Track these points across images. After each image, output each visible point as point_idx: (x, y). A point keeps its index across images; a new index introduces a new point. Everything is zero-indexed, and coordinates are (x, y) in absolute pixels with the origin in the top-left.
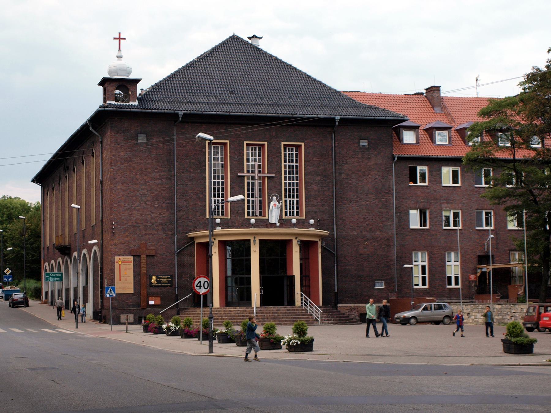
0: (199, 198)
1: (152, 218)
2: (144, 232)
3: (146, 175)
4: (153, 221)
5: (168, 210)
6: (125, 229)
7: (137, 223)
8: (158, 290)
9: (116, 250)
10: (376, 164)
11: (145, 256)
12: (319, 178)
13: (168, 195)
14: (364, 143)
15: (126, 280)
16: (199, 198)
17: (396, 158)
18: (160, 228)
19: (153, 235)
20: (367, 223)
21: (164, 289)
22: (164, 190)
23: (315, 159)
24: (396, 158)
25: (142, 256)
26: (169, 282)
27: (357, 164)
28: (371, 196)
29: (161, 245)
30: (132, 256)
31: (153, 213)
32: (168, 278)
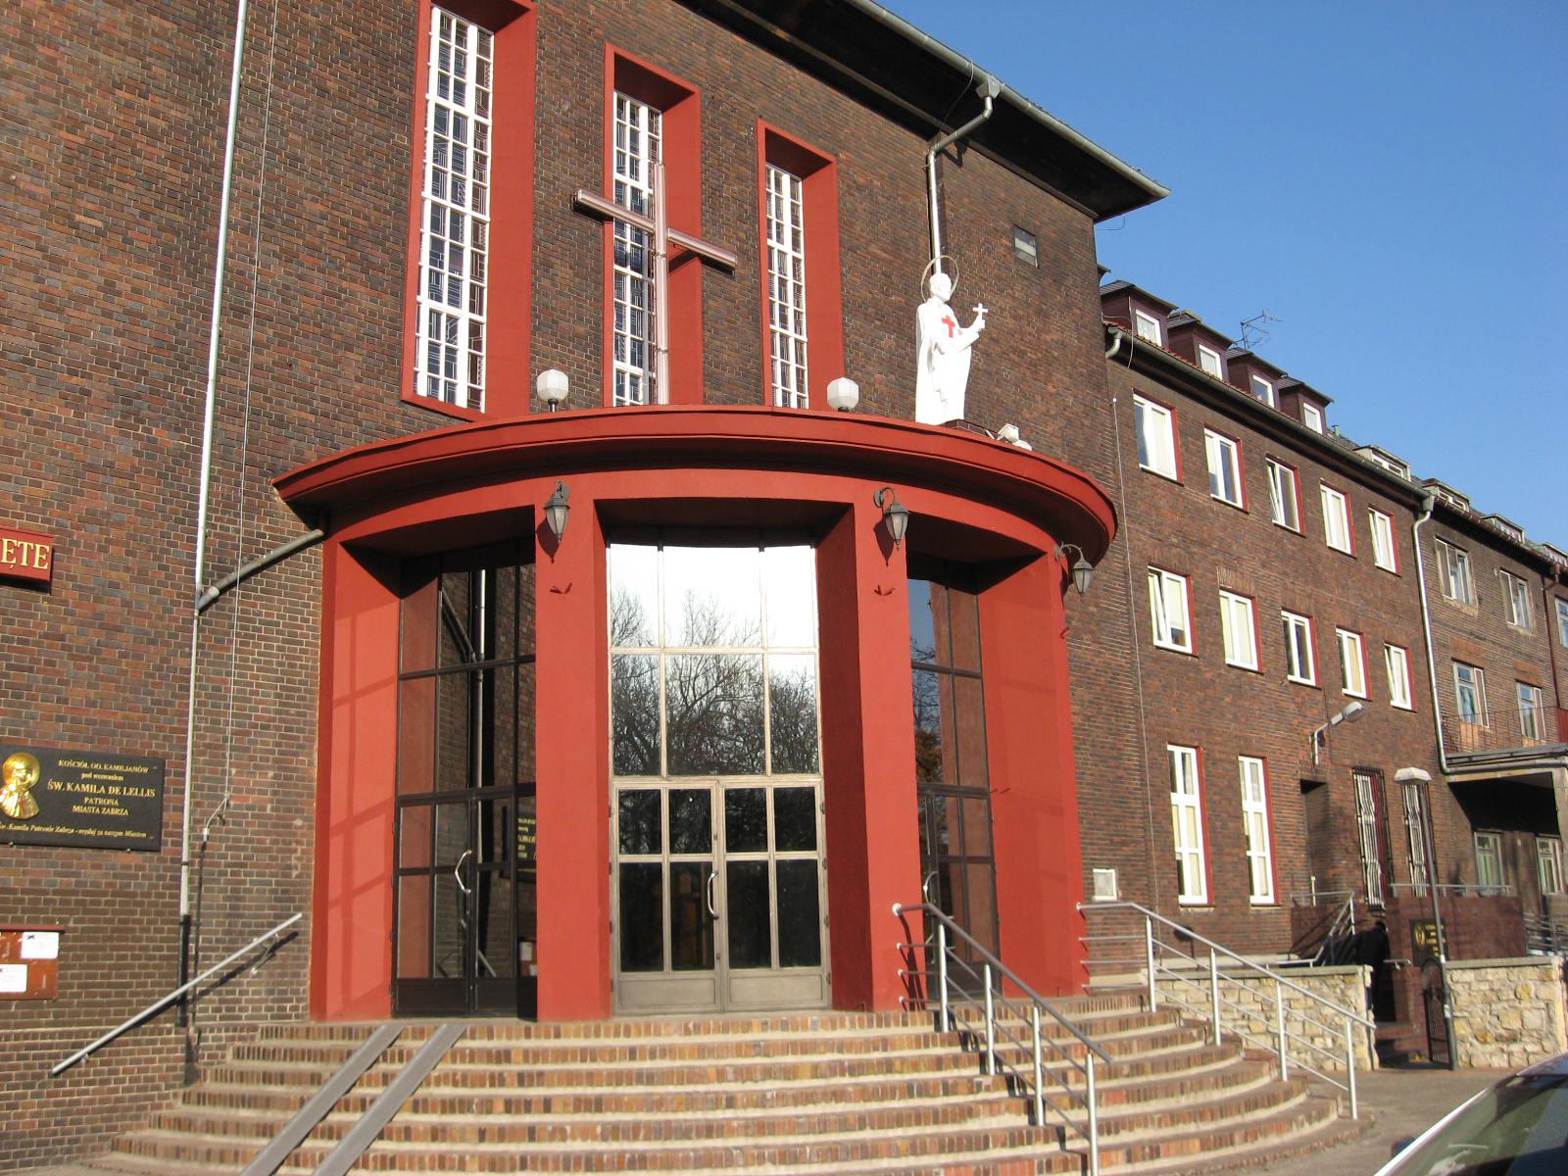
0: (366, 265)
1: (48, 303)
4: (53, 322)
5: (166, 272)
8: (46, 870)
13: (177, 176)
14: (1027, 249)
16: (366, 265)
17: (1117, 343)
19: (42, 426)
21: (92, 869)
22: (154, 135)
23: (874, 249)
24: (1117, 343)
29: (91, 518)
31: (57, 263)
32: (130, 780)
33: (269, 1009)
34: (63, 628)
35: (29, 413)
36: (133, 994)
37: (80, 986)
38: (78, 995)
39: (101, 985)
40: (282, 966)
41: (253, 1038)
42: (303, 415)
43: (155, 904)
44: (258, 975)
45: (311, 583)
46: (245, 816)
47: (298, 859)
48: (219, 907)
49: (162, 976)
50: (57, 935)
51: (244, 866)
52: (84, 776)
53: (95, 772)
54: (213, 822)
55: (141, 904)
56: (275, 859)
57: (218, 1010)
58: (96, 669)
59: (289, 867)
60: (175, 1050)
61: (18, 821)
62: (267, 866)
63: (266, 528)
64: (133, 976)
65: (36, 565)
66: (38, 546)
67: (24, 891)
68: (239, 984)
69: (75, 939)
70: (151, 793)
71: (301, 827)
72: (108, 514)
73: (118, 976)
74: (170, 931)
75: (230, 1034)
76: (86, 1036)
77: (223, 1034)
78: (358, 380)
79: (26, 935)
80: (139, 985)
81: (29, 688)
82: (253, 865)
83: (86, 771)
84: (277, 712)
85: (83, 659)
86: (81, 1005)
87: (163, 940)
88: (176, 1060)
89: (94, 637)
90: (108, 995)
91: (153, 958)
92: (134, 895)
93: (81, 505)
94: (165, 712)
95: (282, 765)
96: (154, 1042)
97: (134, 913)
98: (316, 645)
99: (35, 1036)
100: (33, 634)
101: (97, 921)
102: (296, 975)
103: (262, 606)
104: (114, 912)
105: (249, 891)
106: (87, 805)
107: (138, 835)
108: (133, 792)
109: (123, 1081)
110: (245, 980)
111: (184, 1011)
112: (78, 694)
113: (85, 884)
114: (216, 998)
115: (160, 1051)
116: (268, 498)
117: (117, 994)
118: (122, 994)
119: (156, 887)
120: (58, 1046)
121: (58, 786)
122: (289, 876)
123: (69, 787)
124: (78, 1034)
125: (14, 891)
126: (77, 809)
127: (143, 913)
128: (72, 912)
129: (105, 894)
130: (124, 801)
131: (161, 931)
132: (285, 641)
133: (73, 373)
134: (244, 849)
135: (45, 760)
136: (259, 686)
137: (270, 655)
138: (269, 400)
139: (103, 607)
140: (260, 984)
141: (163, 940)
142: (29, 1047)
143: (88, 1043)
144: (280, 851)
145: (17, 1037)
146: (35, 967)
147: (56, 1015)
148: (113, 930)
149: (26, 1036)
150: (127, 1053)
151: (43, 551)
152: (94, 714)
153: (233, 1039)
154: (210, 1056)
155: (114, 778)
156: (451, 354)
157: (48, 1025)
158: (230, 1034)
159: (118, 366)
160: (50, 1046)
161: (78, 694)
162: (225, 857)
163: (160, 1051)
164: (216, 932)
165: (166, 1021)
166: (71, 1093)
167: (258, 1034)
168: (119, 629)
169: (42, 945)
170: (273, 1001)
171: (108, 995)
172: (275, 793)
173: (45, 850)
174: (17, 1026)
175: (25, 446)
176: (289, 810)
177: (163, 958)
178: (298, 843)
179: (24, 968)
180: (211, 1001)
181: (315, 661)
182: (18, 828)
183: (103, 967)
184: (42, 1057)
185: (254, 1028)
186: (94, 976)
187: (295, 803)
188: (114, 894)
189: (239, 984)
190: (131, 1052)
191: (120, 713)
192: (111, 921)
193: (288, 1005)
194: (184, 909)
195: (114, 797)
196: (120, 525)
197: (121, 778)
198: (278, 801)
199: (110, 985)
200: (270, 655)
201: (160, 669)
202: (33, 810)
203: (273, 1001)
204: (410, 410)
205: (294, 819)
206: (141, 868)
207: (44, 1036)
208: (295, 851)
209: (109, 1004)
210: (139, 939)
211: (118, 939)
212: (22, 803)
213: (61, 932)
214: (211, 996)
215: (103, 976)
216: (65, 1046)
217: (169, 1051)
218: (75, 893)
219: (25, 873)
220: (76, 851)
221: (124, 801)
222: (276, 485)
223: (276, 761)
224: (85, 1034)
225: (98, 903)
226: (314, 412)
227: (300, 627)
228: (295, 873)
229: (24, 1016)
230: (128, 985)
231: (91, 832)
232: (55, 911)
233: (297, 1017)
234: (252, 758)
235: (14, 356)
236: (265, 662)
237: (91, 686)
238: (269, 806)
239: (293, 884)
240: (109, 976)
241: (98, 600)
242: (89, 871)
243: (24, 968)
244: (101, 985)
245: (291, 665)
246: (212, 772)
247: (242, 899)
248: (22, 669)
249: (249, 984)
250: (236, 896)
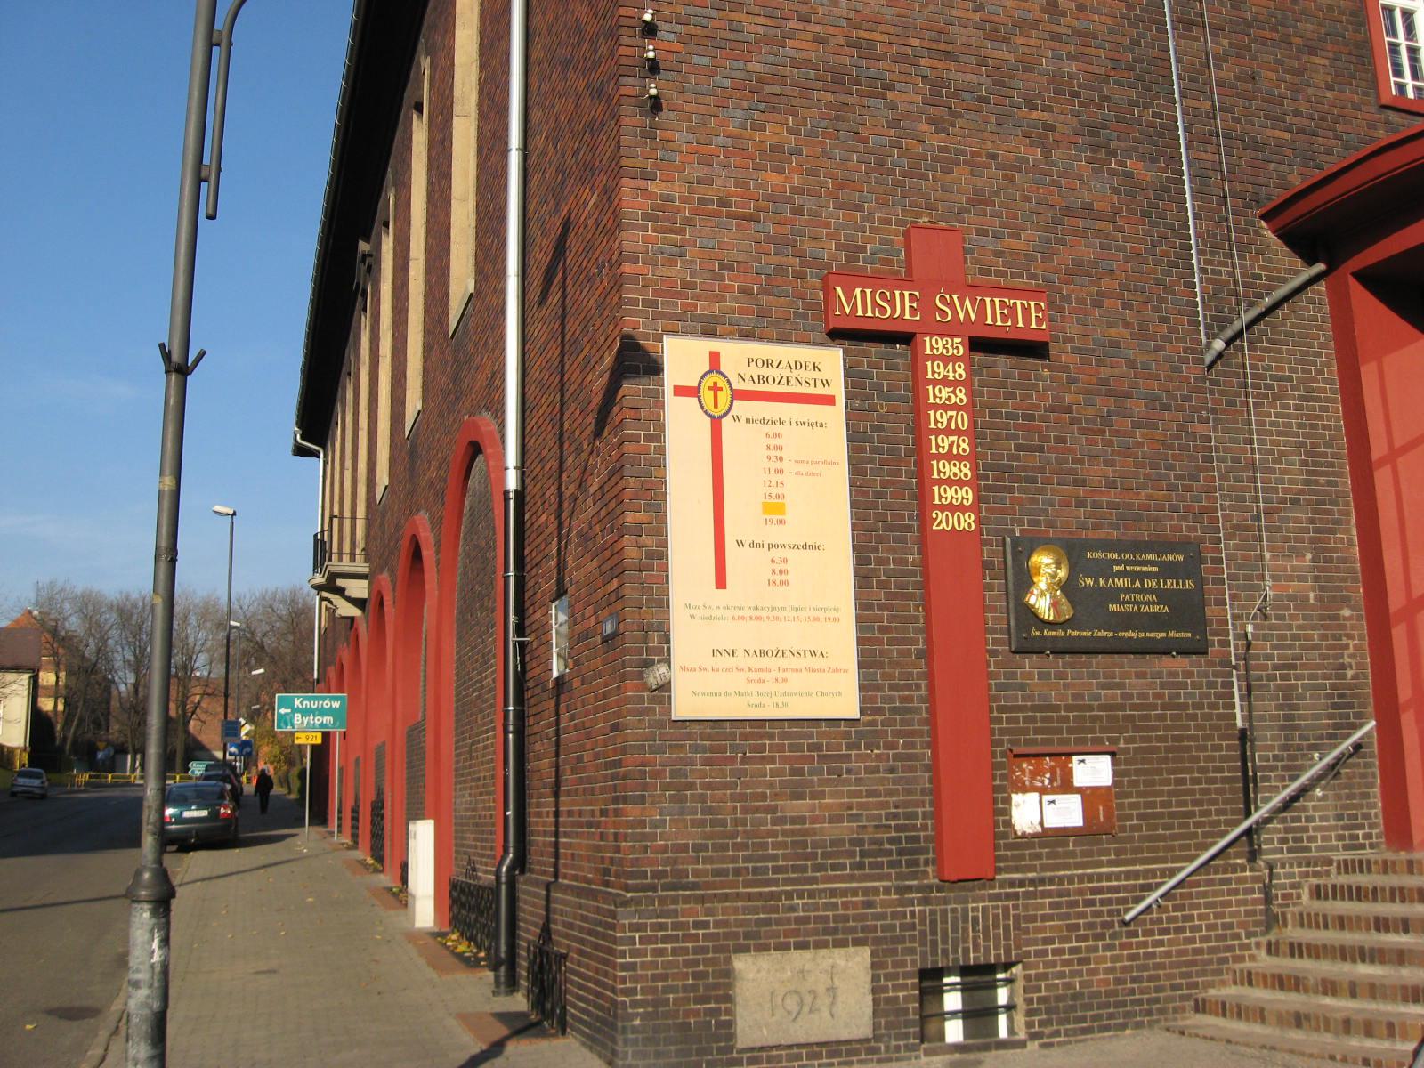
2: (934, 140)
4: (1003, 53)
6: (754, 88)
7: (868, 51)
8: (1088, 681)
9: (678, 273)
15: (779, 578)
18: (1064, 123)
25: (934, 344)
29: (1077, 270)
30: (837, 335)
32: (1168, 571)
33: (1341, 838)
34: (1068, 398)
35: (993, 157)
36: (1198, 825)
37: (1141, 817)
38: (1138, 828)
39: (1161, 816)
40: (1346, 786)
41: (1328, 873)
42: (1277, 133)
43: (1209, 717)
44: (1324, 798)
45: (1320, 328)
46: (1287, 608)
47: (1351, 656)
48: (1273, 718)
49: (1226, 802)
50: (1107, 758)
51: (1294, 667)
52: (1116, 568)
53: (1127, 563)
54: (1255, 617)
55: (1194, 718)
56: (1326, 657)
57: (1284, 841)
58: (1110, 443)
59: (1343, 667)
60: (1252, 891)
61: (1052, 625)
62: (1318, 667)
63: (1261, 268)
64: (1196, 803)
65: (1034, 326)
66: (1032, 304)
67: (1068, 708)
68: (1304, 809)
69: (1127, 762)
70: (1190, 585)
71: (1350, 618)
72: (1094, 264)
73: (1180, 804)
74: (1229, 748)
75: (1303, 869)
76: (1154, 877)
77: (1296, 870)
78: (1330, 88)
79: (1075, 758)
80: (1203, 814)
81: (1042, 470)
82: (1303, 666)
83: (1118, 563)
84: (1306, 482)
85: (1095, 433)
86: (1142, 839)
87: (1223, 759)
88: (1255, 902)
89: (1103, 405)
90: (1170, 827)
91: (1214, 781)
92: (1185, 707)
93: (1065, 256)
94: (1190, 489)
95: (1318, 545)
96: (1228, 881)
97: (1187, 728)
98: (1334, 401)
99: (1100, 877)
100: (1038, 407)
101: (1149, 739)
102: (1366, 796)
103: (1271, 359)
104: (1167, 728)
105: (1303, 697)
106: (1124, 602)
107: (1183, 635)
108: (1170, 584)
109: (1199, 928)
110: (1310, 804)
111: (1251, 843)
112: (1096, 472)
113: (1130, 696)
114: (1281, 826)
115: (1236, 892)
116: (1257, 233)
117: (1181, 826)
118: (1186, 826)
119: (1208, 696)
120: (1126, 889)
121: (1090, 582)
122: (1344, 677)
123: (1102, 582)
124: (1147, 874)
125: (1056, 708)
126: (1113, 608)
127: (1198, 728)
128: (1120, 730)
129: (1154, 707)
131: (1219, 748)
132: (1302, 398)
133: (1032, 108)
134: (1291, 647)
135: (1072, 552)
136: (1281, 453)
137: (1288, 416)
138: (1238, 120)
139: (1106, 371)
140: (1326, 808)
141: (1223, 759)
142: (1095, 891)
143: (1159, 885)
144: (1330, 648)
145: (1081, 879)
146: (1091, 796)
147: (1118, 852)
148: (1168, 750)
149: (1090, 878)
150: (1200, 895)
151: (1038, 307)
152: (1114, 495)
153: (1307, 875)
154: (1285, 897)
155: (1149, 569)
157: (1111, 863)
158: (1303, 869)
159: (1077, 95)
160: (1116, 890)
161: (1096, 472)
162: (1271, 658)
163: (1236, 892)
164: (1272, 748)
165: (1237, 856)
166: (1145, 944)
167: (1333, 869)
168: (1128, 395)
169: (1094, 771)
170: (1343, 828)
171: (1170, 827)
172: (1316, 579)
173: (1084, 658)
174: (1078, 866)
175: (996, 194)
176: (1334, 598)
177: (1224, 780)
178: (1350, 637)
179: (1077, 798)
180: (1277, 831)
181: (1337, 420)
182: (1054, 634)
183: (1160, 793)
184: (1110, 902)
185: (1329, 862)
186: (1153, 805)
187: (1339, 589)
188: (1164, 707)
189: (1304, 809)
190: (1205, 894)
191: (1143, 493)
192: (1163, 739)
193: (1361, 833)
194: (1239, 723)
195: (1151, 591)
196: (1110, 274)
197: (1156, 569)
198: (1322, 589)
199: (1172, 815)
200: (1288, 416)
201: (1178, 438)
202: (1067, 612)
203: (1343, 828)
204: (1392, 116)
205: (1340, 608)
206: (1189, 674)
207: (1109, 877)
208: (1346, 647)
209: (1174, 837)
210: (1197, 759)
211: (1175, 760)
212: (1055, 605)
213: (1113, 754)
214: (1275, 825)
215: (1163, 804)
216: (1134, 888)
217: (1246, 891)
218: (1122, 707)
219: (1066, 686)
220: (1117, 658)
222: (1263, 217)
223: (1312, 540)
224: (1153, 873)
225: (1147, 718)
226: (1288, 130)
227: (1315, 381)
228: (1350, 673)
229: (1083, 854)
230: (1190, 814)
231: (1131, 634)
232: (1104, 729)
233: (1372, 846)
234: (1287, 539)
235: (967, 95)
236: (1285, 425)
237: (1108, 463)
238: (1312, 595)
239: (1350, 687)
240: (1169, 804)
241: (1100, 363)
242: (1134, 681)
243: (1077, 798)
244: (1161, 816)
245: (1313, 426)
246: (1245, 558)
247: (1296, 707)
248: (1031, 449)
249: (1315, 808)
250: (1289, 703)
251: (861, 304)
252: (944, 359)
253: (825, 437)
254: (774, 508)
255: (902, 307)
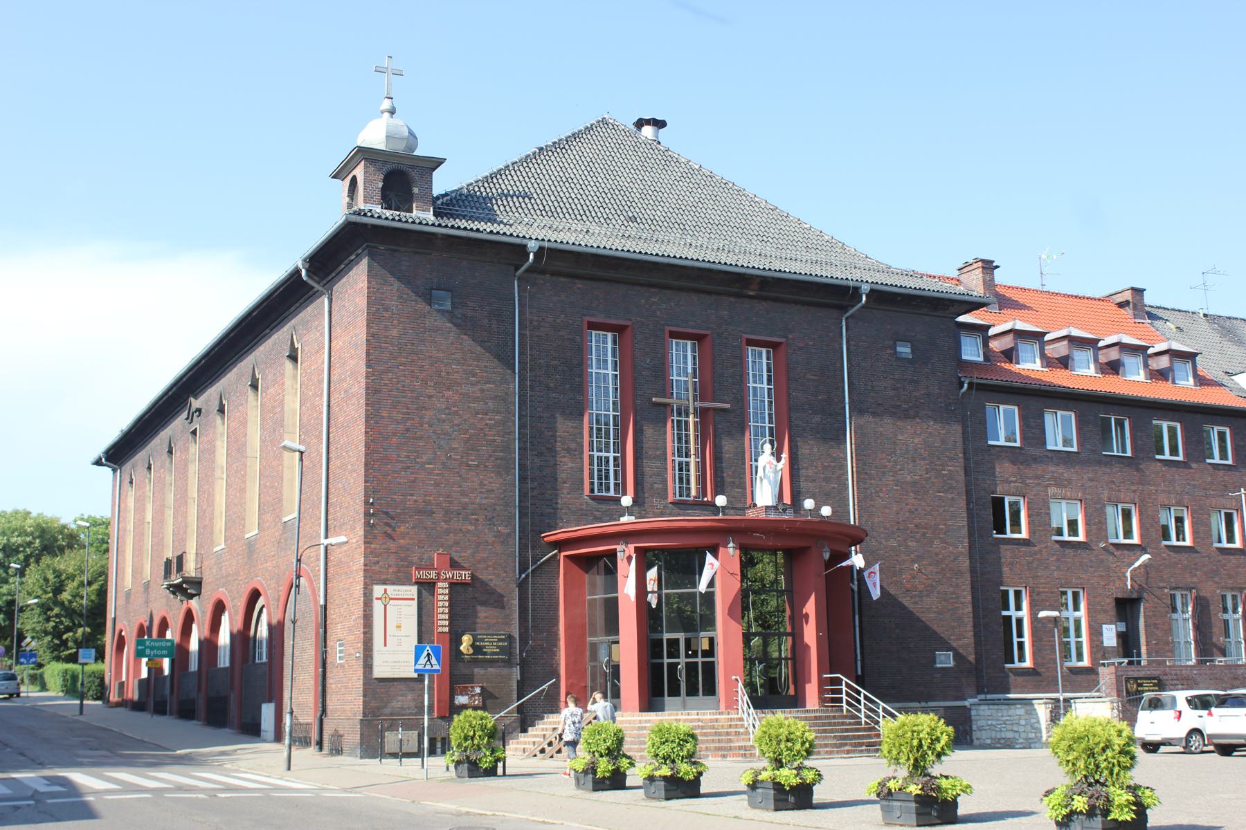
3: (448, 389)
5: (499, 474)
7: (428, 503)
9: (377, 568)
10: (928, 395)
11: (446, 585)
12: (817, 418)
13: (499, 439)
14: (905, 350)
15: (400, 644)
17: (966, 386)
18: (481, 518)
20: (917, 521)
23: (809, 376)
24: (966, 386)
25: (440, 584)
26: (503, 650)
27: (892, 393)
28: (923, 463)
30: (416, 583)
32: (500, 640)
130: (498, 647)
156: (607, 471)
221: (498, 647)
251: (423, 575)
252: (442, 589)
253: (410, 610)
254: (399, 627)
255: (433, 575)
